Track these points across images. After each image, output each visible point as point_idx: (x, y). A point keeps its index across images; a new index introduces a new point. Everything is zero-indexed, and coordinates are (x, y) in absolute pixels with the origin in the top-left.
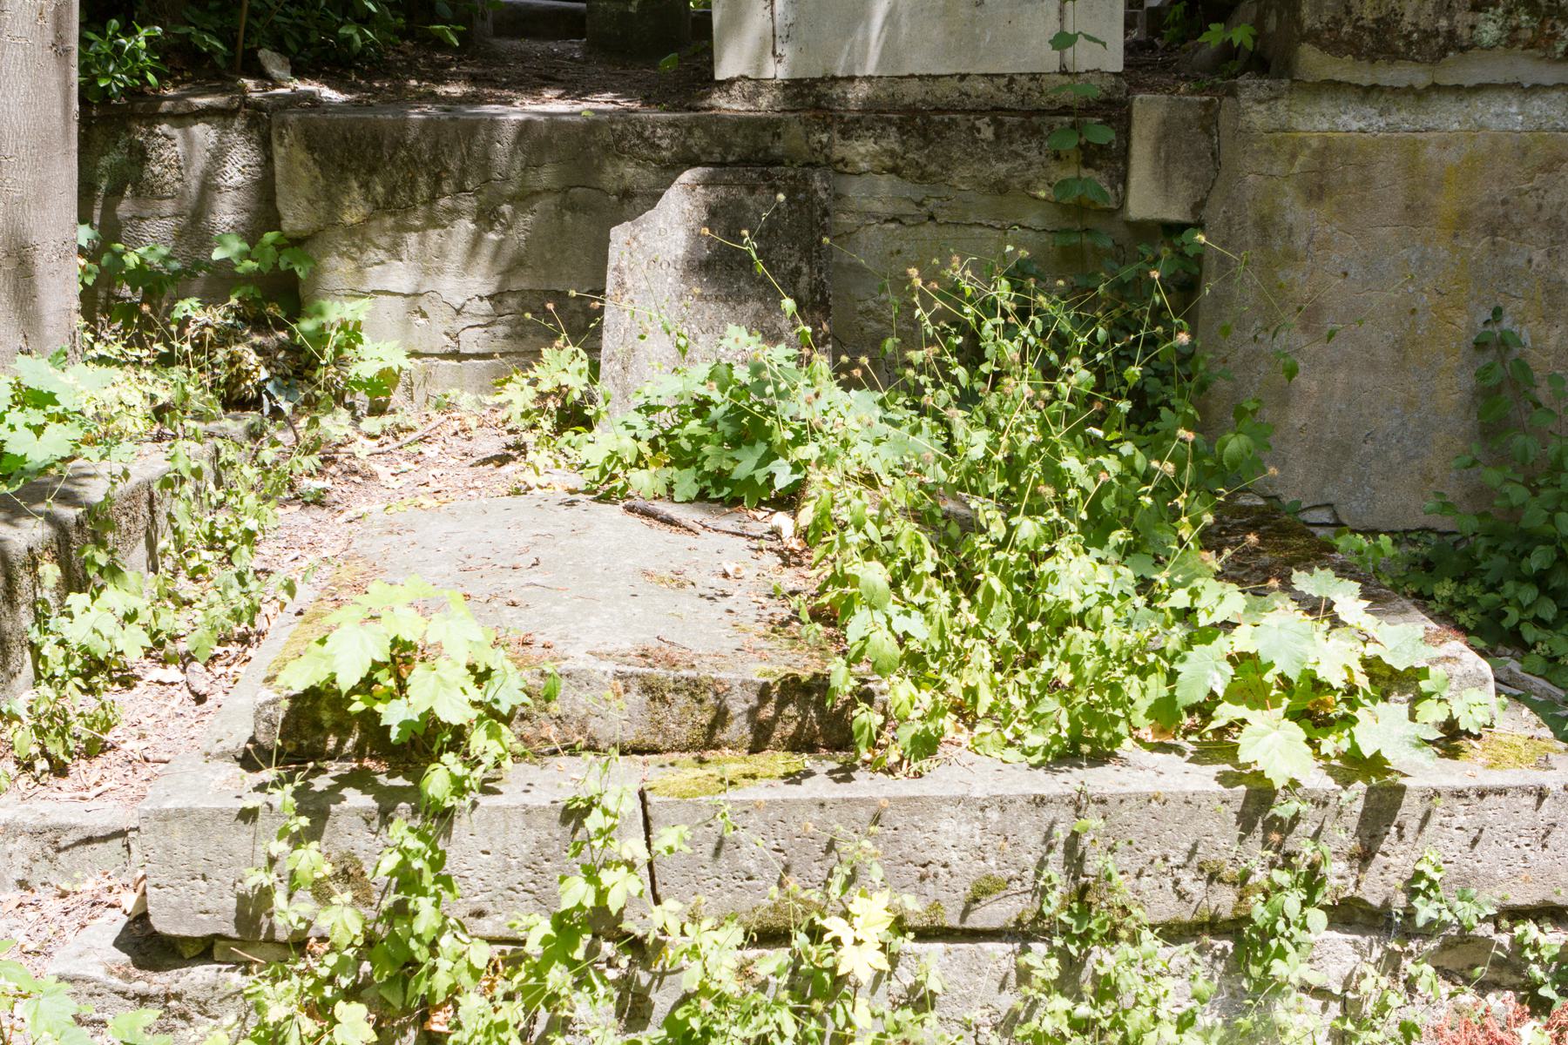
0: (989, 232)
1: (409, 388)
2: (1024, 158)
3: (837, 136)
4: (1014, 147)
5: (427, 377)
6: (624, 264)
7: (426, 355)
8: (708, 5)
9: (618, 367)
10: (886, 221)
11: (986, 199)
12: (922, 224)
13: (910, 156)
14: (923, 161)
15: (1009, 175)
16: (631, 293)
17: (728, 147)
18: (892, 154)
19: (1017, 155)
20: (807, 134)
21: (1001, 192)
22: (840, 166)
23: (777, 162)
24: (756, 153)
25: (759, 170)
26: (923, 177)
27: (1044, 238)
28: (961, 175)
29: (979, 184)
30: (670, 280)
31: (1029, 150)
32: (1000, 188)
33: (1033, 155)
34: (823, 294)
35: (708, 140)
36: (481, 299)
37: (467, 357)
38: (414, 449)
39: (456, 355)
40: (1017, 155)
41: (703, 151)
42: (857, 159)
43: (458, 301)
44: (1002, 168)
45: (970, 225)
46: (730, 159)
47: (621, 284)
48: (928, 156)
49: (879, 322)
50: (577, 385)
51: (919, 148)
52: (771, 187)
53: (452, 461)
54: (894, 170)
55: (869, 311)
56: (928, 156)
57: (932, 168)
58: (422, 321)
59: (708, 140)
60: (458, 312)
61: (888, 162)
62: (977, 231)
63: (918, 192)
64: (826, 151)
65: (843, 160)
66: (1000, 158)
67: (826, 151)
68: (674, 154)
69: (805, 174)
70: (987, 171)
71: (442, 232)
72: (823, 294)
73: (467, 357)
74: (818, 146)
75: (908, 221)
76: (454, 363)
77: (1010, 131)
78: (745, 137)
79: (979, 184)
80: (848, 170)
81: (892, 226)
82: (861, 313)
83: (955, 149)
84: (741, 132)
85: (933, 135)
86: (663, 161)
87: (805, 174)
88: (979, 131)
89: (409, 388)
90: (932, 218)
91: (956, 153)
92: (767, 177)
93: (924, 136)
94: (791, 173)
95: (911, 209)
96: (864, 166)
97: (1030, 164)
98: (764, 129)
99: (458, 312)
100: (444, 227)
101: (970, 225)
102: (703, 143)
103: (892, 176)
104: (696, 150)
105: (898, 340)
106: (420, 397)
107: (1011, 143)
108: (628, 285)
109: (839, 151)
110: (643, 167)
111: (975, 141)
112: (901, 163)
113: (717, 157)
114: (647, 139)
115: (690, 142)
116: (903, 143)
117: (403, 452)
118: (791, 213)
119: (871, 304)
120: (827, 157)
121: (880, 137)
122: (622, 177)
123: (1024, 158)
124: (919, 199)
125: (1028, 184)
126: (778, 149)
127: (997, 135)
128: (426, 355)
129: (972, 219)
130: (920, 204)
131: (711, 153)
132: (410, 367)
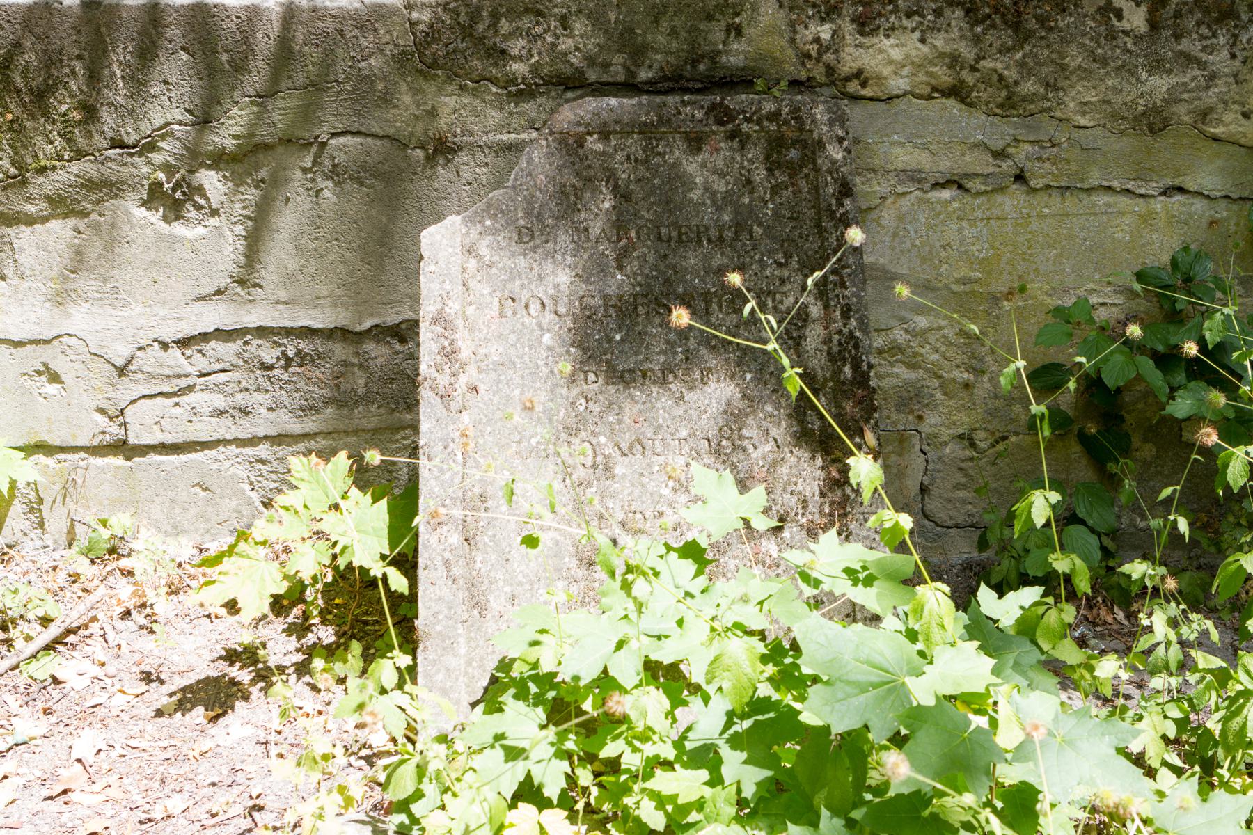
0: (1123, 201)
1: (35, 507)
2: (1202, 65)
3: (849, 28)
4: (1184, 45)
5: (67, 490)
6: (453, 307)
7: (63, 449)
8: (1233, 3)
9: (455, 539)
10: (936, 185)
11: (1123, 144)
12: (1001, 189)
13: (987, 64)
14: (1011, 74)
15: (1172, 98)
16: (472, 370)
17: (638, 53)
18: (954, 61)
19: (1188, 59)
20: (793, 25)
21: (1153, 131)
22: (853, 87)
23: (740, 81)
24: (695, 63)
25: (706, 100)
26: (1010, 104)
27: (1222, 211)
28: (1080, 98)
29: (1114, 116)
30: (547, 339)
31: (1209, 50)
32: (1153, 122)
33: (1220, 60)
34: (856, 365)
35: (600, 39)
36: (165, 346)
37: (143, 450)
38: (44, 667)
39: (121, 447)
40: (1188, 59)
41: (591, 61)
42: (886, 71)
43: (120, 352)
44: (1159, 85)
45: (1089, 190)
46: (644, 75)
47: (450, 353)
48: (1022, 64)
49: (912, 366)
50: (364, 534)
51: (1005, 50)
52: (732, 136)
53: (120, 700)
54: (956, 92)
55: (895, 349)
56: (1022, 64)
57: (1028, 87)
58: (52, 389)
59: (600, 39)
60: (121, 371)
61: (945, 77)
62: (1102, 200)
63: (1000, 132)
64: (829, 57)
65: (858, 74)
66: (1157, 66)
67: (829, 57)
68: (535, 70)
69: (796, 109)
70: (1130, 92)
71: (81, 223)
72: (856, 365)
73: (143, 450)
74: (813, 49)
75: (976, 185)
76: (118, 461)
77: (1178, 15)
78: (674, 32)
79: (1114, 116)
80: (866, 92)
81: (946, 194)
82: (880, 352)
83: (1073, 50)
84: (665, 24)
85: (1032, 24)
86: (513, 81)
87: (796, 109)
88: (1119, 15)
89: (35, 507)
90: (1020, 178)
91: (1075, 58)
92: (722, 115)
93: (1016, 26)
94: (769, 106)
95: (984, 164)
96: (899, 84)
97: (1212, 77)
98: (710, 18)
99: (121, 371)
100: (84, 214)
101: (1089, 190)
102: (591, 45)
103: (951, 103)
104: (576, 59)
105: (1055, 497)
106: (56, 524)
107: (1178, 37)
108: (465, 354)
109: (854, 57)
110: (474, 93)
111: (1112, 35)
112: (969, 78)
113: (618, 73)
114: (481, 39)
115: (566, 44)
116: (977, 40)
117: (21, 679)
118: (775, 190)
119: (900, 336)
120: (830, 70)
121: (934, 28)
122: (433, 113)
123: (1202, 65)
124: (998, 145)
125: (1205, 114)
126: (736, 55)
127: (1154, 25)
128: (63, 449)
129: (1095, 178)
130: (1000, 155)
131: (606, 66)
132: (33, 476)
